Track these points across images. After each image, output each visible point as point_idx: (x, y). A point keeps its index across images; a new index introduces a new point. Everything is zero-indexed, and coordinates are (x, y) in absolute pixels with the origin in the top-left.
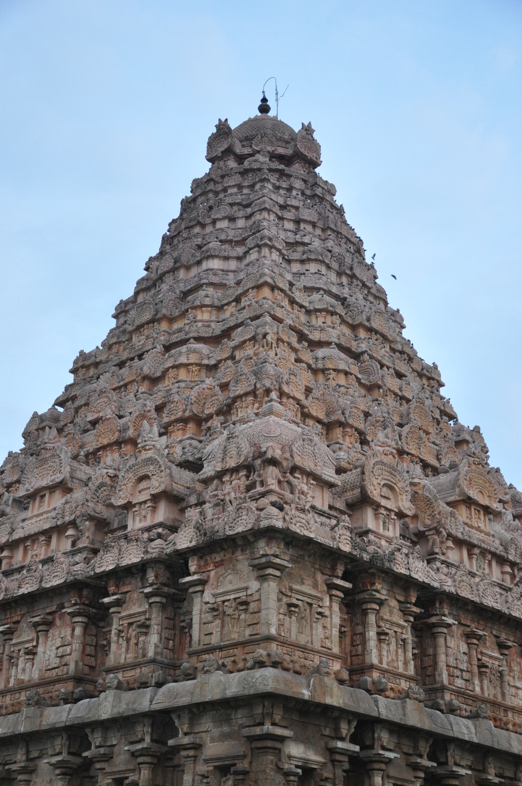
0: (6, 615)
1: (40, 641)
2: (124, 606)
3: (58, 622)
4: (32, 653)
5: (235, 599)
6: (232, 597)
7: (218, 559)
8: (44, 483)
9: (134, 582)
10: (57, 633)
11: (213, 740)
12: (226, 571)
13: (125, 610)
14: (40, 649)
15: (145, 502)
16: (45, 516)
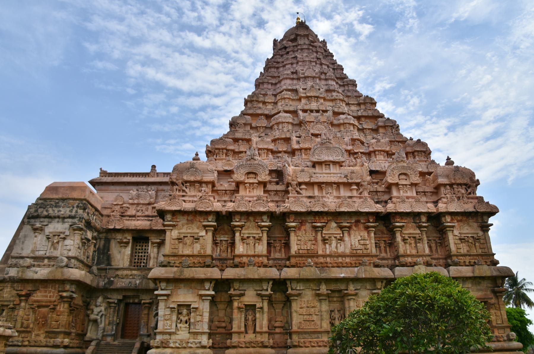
0: (315, 218)
1: (346, 234)
2: (404, 228)
3: (354, 227)
4: (341, 239)
5: (471, 237)
6: (470, 235)
7: (459, 219)
8: (331, 159)
9: (409, 219)
10: (357, 233)
11: (473, 291)
12: (464, 224)
13: (405, 230)
14: (346, 238)
15: (406, 185)
16: (332, 175)
